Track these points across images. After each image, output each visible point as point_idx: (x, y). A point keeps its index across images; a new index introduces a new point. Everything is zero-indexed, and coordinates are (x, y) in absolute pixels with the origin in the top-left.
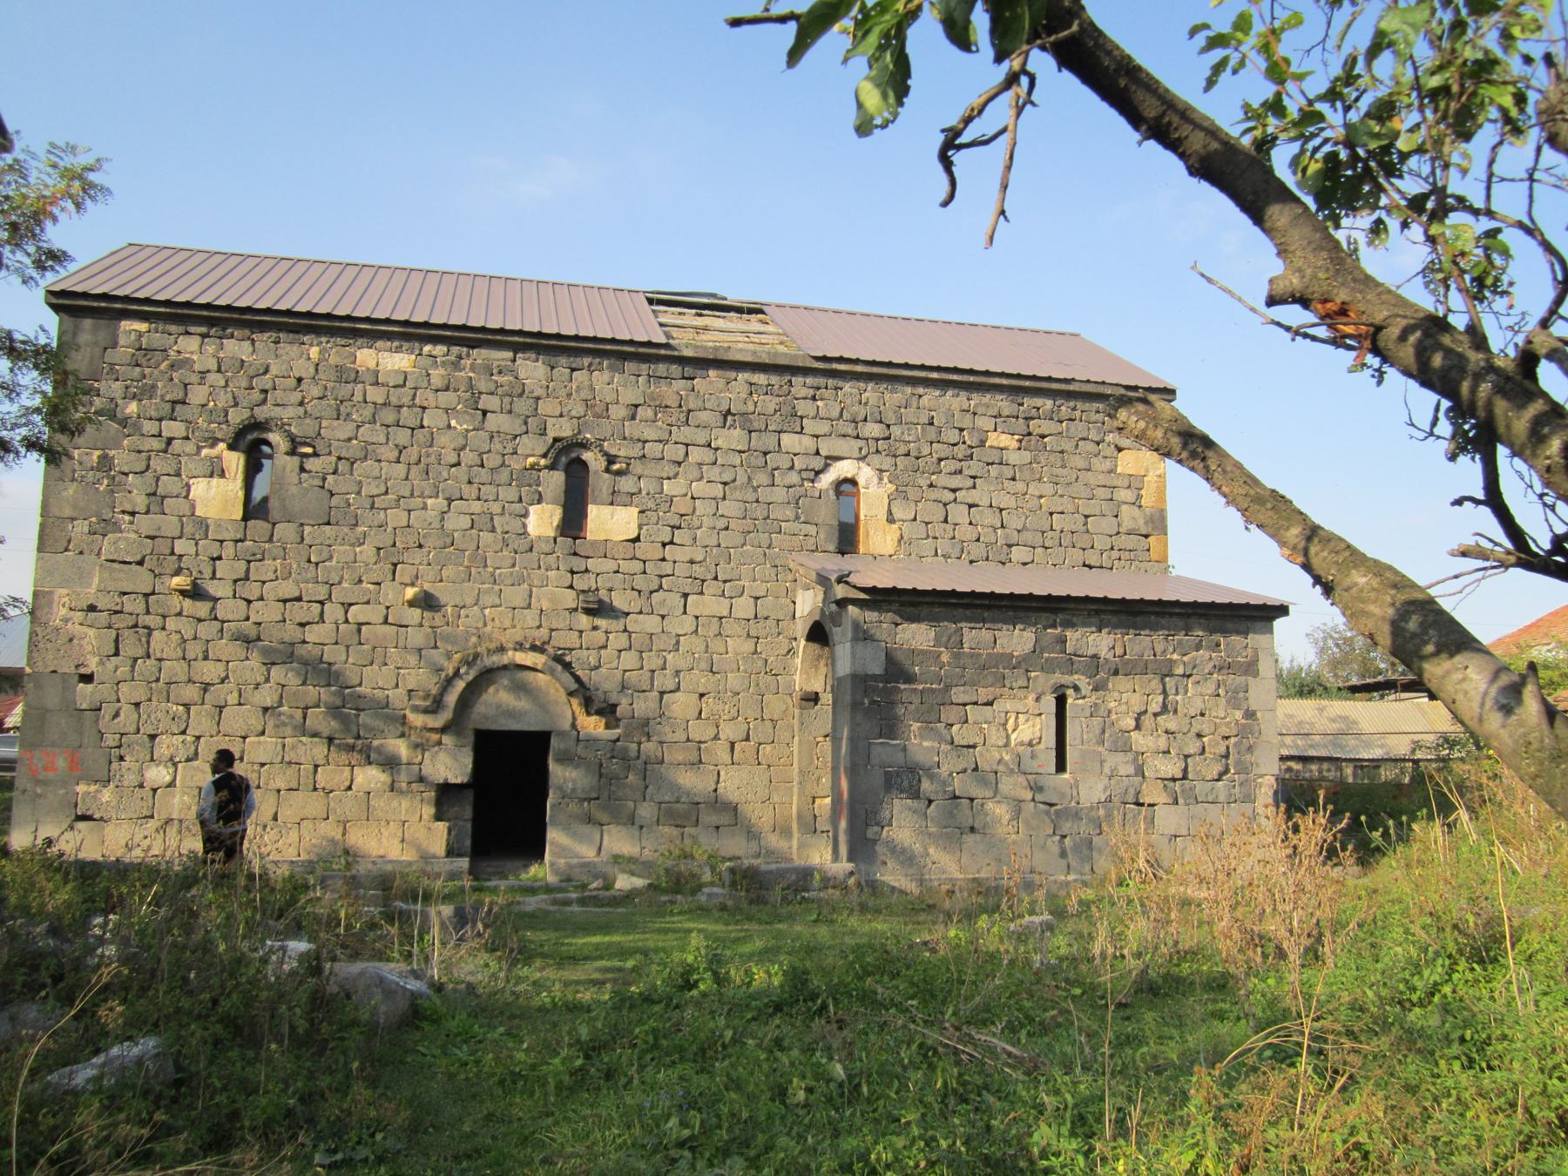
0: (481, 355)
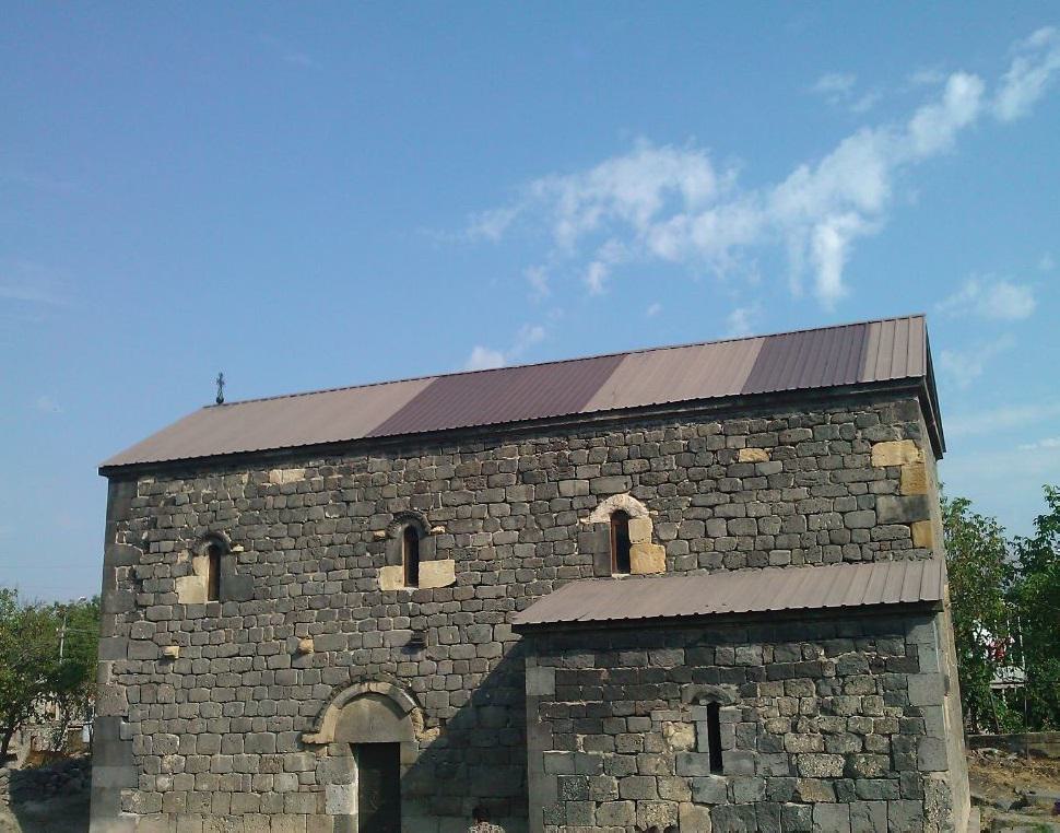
0: (340, 463)
